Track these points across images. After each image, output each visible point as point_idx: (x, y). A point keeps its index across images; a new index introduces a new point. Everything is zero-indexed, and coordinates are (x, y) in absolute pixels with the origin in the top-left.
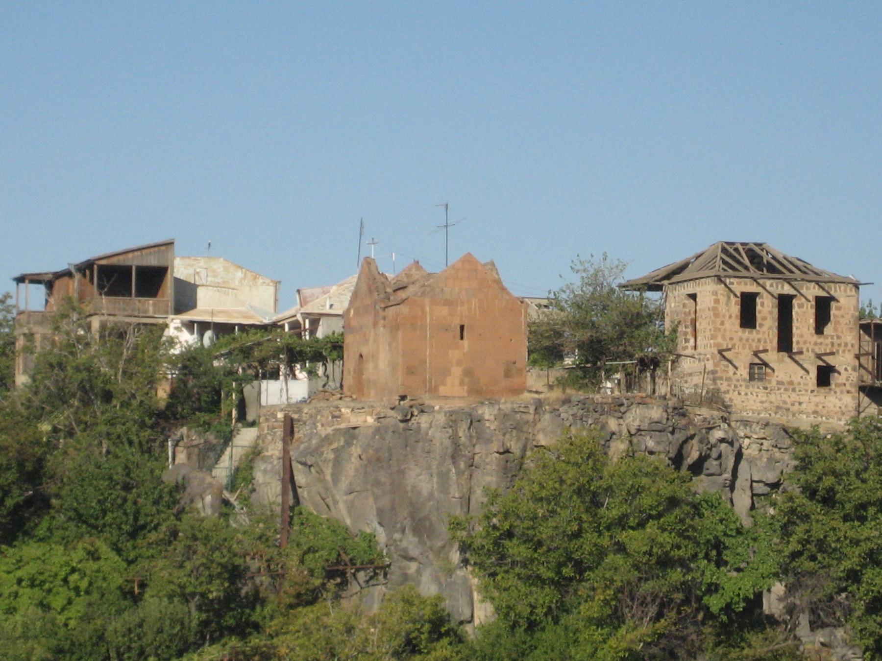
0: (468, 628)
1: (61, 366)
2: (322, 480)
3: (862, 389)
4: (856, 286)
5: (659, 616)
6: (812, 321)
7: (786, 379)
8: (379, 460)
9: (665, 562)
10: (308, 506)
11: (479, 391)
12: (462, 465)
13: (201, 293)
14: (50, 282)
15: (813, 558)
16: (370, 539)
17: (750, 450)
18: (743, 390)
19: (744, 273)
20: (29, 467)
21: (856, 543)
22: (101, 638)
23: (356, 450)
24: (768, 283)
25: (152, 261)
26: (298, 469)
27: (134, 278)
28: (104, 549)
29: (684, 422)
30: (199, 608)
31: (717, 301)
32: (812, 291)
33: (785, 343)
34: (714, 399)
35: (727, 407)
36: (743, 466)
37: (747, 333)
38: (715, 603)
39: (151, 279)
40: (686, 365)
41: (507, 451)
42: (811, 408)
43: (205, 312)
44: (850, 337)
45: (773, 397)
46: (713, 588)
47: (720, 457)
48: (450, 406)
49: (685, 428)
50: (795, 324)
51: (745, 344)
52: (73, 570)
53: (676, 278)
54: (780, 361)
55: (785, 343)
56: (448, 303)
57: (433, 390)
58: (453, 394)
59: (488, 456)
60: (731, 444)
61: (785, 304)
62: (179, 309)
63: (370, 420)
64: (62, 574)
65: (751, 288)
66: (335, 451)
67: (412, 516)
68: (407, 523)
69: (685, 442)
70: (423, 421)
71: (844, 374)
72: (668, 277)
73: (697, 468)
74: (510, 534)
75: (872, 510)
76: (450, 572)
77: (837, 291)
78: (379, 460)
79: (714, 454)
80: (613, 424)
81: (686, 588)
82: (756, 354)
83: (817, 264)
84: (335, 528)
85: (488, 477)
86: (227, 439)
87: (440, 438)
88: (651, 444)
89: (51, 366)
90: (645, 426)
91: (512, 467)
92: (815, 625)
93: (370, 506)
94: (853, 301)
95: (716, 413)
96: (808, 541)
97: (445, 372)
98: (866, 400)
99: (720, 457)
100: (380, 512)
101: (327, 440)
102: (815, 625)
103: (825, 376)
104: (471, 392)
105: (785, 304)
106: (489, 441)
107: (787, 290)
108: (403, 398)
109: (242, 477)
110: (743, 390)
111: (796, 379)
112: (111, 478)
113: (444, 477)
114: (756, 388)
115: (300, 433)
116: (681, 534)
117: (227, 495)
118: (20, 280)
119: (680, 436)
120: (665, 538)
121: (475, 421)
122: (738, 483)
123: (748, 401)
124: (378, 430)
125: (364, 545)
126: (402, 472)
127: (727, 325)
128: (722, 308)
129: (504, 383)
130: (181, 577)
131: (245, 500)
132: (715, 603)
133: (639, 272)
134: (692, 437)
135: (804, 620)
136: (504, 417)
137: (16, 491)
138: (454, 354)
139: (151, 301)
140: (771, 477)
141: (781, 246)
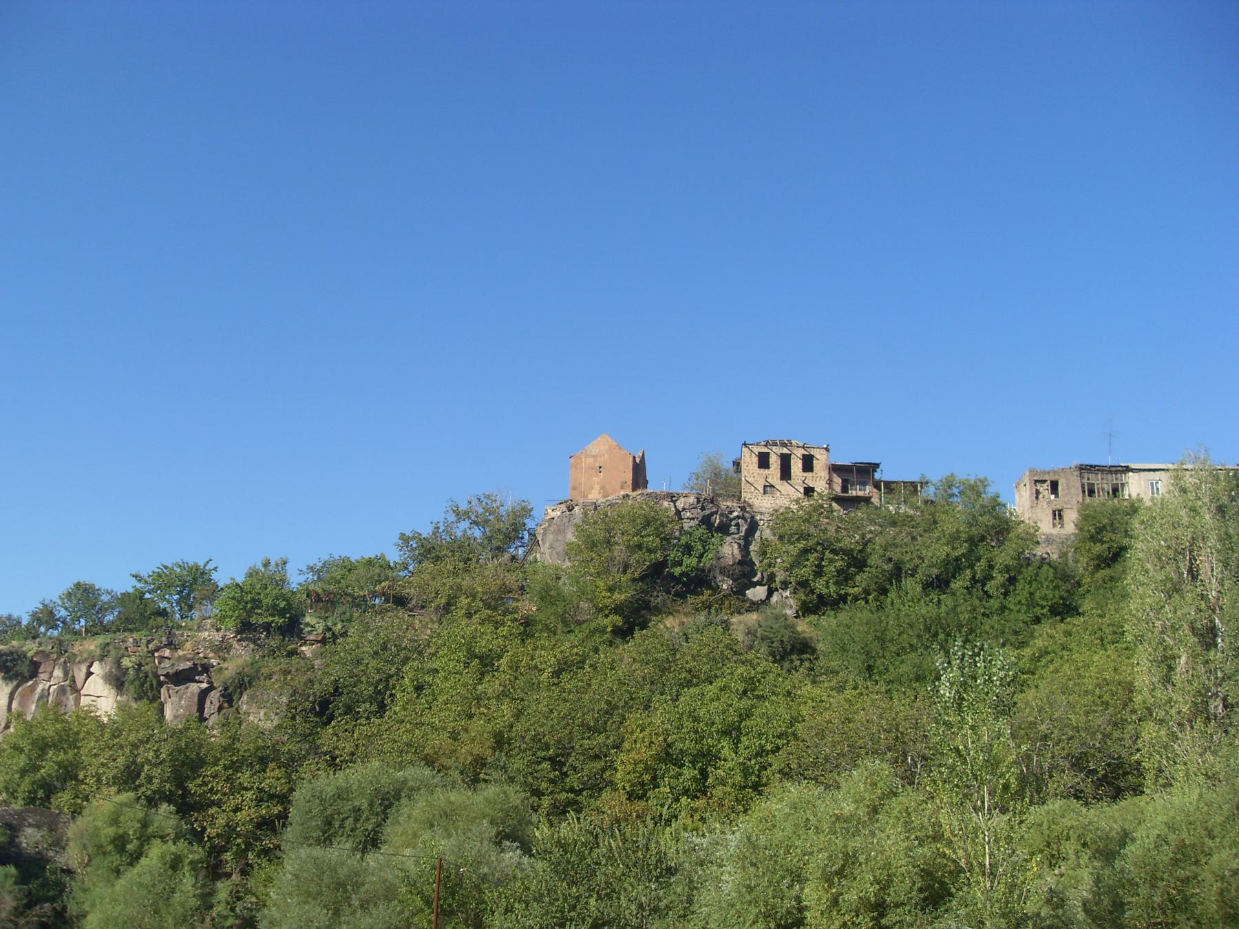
6: (800, 465)
32: (802, 452)
55: (786, 474)
57: (585, 496)
60: (743, 518)
61: (785, 461)
73: (724, 529)
98: (834, 504)
99: (737, 525)
105: (785, 461)
107: (785, 451)
114: (767, 497)
119: (707, 512)
134: (716, 513)
138: (596, 479)
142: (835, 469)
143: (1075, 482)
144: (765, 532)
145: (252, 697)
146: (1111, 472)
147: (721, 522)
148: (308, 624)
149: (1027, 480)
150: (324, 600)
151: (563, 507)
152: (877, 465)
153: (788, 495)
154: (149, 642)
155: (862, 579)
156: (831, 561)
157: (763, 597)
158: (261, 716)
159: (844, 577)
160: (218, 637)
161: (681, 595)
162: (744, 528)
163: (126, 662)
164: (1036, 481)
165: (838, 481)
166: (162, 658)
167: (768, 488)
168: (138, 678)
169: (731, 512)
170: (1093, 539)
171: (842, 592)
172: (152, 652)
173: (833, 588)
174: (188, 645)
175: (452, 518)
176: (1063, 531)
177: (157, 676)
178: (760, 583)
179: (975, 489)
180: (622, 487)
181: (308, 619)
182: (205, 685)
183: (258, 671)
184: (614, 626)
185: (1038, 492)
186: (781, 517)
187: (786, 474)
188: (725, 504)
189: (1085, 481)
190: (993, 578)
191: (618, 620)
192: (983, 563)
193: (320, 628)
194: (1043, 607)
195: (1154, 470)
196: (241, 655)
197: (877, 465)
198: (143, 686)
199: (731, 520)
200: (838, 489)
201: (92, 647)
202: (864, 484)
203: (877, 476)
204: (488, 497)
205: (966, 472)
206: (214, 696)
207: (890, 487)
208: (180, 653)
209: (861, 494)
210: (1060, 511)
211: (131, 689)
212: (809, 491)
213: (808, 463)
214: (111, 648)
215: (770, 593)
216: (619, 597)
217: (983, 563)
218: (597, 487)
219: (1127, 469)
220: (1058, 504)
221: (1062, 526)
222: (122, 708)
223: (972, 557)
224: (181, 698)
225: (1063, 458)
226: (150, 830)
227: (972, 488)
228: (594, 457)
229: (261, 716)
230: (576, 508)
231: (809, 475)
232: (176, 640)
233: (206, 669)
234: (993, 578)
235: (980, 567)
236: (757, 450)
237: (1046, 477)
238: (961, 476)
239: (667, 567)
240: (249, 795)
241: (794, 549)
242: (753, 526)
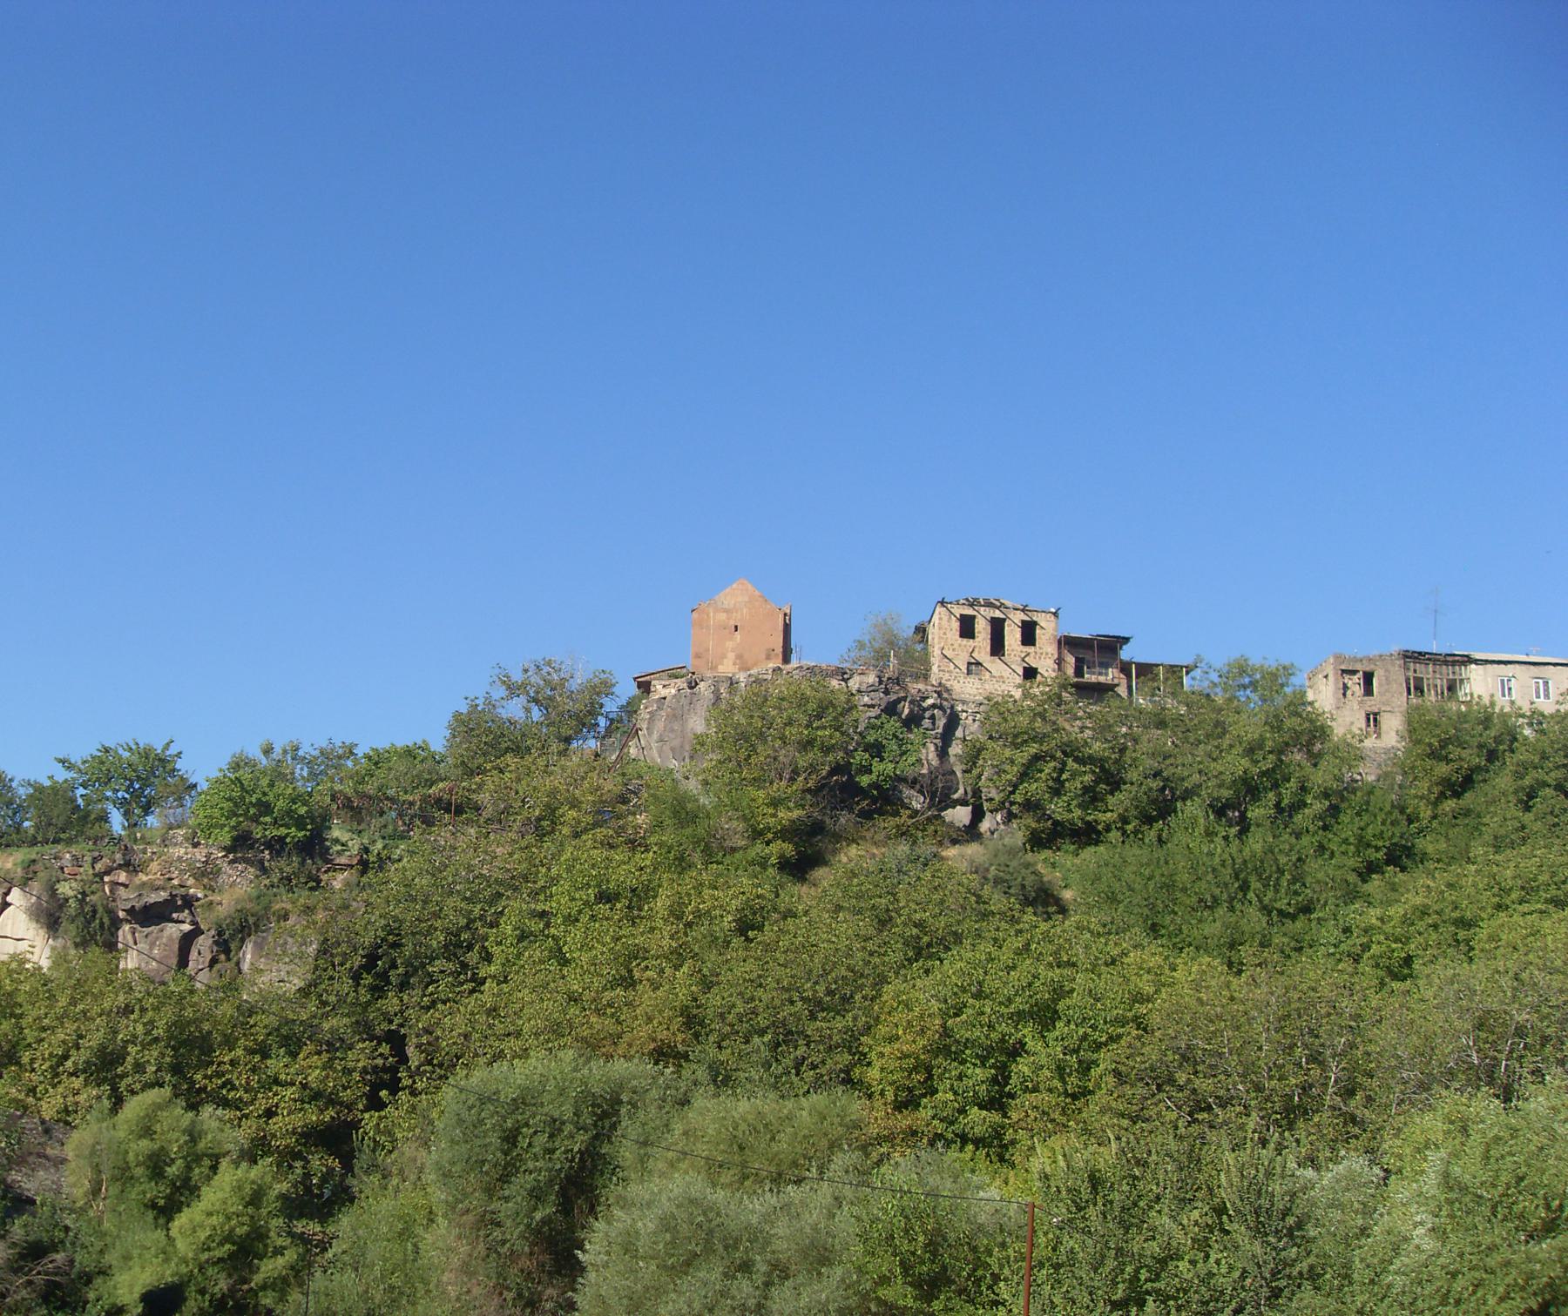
6: (1019, 636)
32: (1019, 617)
37: (965, 641)
38: (865, 780)
44: (1052, 650)
46: (868, 770)
55: (997, 647)
56: (726, 611)
57: (714, 668)
60: (941, 708)
61: (997, 627)
77: (1040, 619)
90: (863, 688)
93: (666, 748)
97: (723, 656)
99: (933, 717)
105: (997, 627)
107: (998, 614)
114: (971, 679)
119: (893, 697)
123: (967, 690)
127: (949, 635)
132: (865, 780)
134: (904, 699)
138: (729, 644)
142: (1067, 643)
143: (1398, 675)
144: (970, 727)
145: (259, 946)
146: (1446, 663)
147: (911, 711)
148: (337, 841)
149: (1330, 670)
150: (355, 810)
151: (682, 683)
152: (1126, 640)
153: (1003, 679)
154: (95, 860)
155: (1119, 802)
156: (1074, 775)
157: (966, 820)
158: (273, 973)
159: (1091, 797)
160: (200, 854)
161: (867, 815)
162: (941, 722)
163: (65, 889)
164: (1343, 671)
165: (1070, 659)
166: (115, 884)
167: (974, 666)
168: (81, 912)
169: (924, 699)
170: (1436, 755)
171: (1089, 818)
172: (101, 875)
173: (1078, 812)
174: (154, 866)
175: (501, 692)
176: (1379, 744)
177: (111, 913)
178: (964, 803)
179: (1274, 680)
180: (768, 658)
181: (336, 833)
182: (187, 927)
183: (267, 908)
184: (781, 856)
185: (1345, 687)
186: (996, 707)
187: (997, 647)
188: (915, 687)
189: (1411, 674)
190: (1305, 805)
191: (788, 849)
192: (1293, 784)
193: (355, 846)
194: (1377, 849)
195: (1487, 662)
196: (237, 886)
197: (1126, 640)
198: (89, 925)
199: (925, 710)
200: (1070, 671)
201: (9, 865)
202: (1106, 666)
203: (1126, 654)
204: (549, 664)
205: (1263, 656)
206: (204, 944)
207: (1146, 670)
208: (143, 877)
209: (1102, 679)
210: (1375, 714)
211: (70, 929)
212: (1030, 673)
213: (1029, 634)
214: (39, 867)
215: (978, 815)
216: (787, 815)
217: (1293, 784)
218: (731, 656)
219: (1468, 660)
220: (1372, 704)
221: (1379, 737)
222: (59, 959)
223: (1276, 777)
224: (152, 945)
225: (1381, 641)
226: (201, 1145)
227: (1274, 676)
228: (726, 611)
229: (273, 973)
230: (702, 685)
232: (136, 860)
233: (189, 902)
234: (1305, 805)
235: (1288, 792)
236: (959, 611)
237: (1358, 667)
238: (1255, 660)
239: (843, 776)
240: (289, 1092)
241: (1022, 757)
242: (953, 721)
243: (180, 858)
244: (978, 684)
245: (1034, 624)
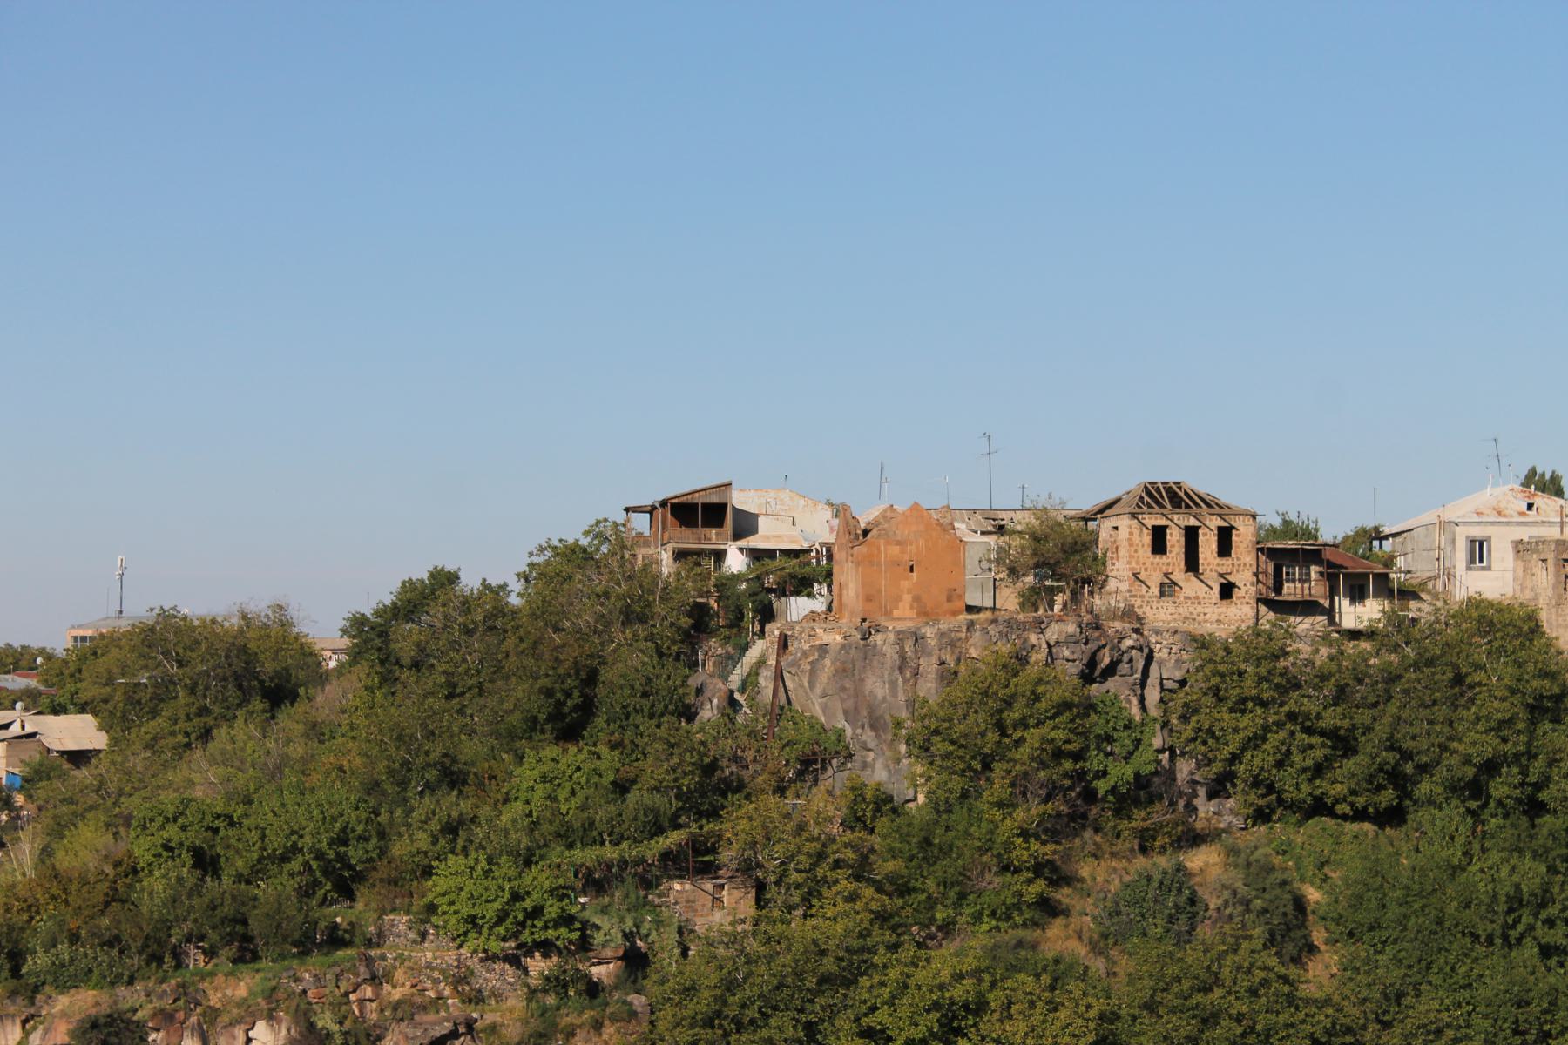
0: (911, 805)
1: (606, 595)
2: (802, 686)
3: (1261, 600)
4: (1254, 517)
5: (1048, 798)
6: (1214, 546)
7: (1192, 594)
8: (844, 670)
9: (1058, 755)
10: (796, 706)
11: (926, 614)
12: (908, 675)
13: (761, 521)
14: (652, 510)
15: (1205, 743)
16: (840, 734)
17: (1161, 653)
18: (1155, 605)
19: (1157, 509)
20: (583, 675)
21: (1236, 730)
22: (592, 824)
23: (828, 662)
24: (1176, 517)
25: (714, 499)
26: (786, 675)
27: (700, 512)
28: (603, 749)
29: (1097, 634)
30: (677, 797)
31: (1131, 534)
32: (1215, 522)
33: (1192, 564)
34: (1129, 614)
35: (1140, 620)
36: (1154, 668)
37: (1157, 558)
39: (714, 513)
40: (1112, 585)
41: (942, 663)
42: (1215, 617)
43: (767, 538)
44: (1249, 559)
45: (1181, 610)
46: (1105, 773)
47: (1131, 660)
48: (901, 626)
49: (1098, 639)
50: (1200, 550)
51: (1155, 568)
52: (579, 769)
53: (1108, 512)
54: (1188, 580)
55: (1192, 564)
56: (899, 543)
57: (888, 614)
58: (904, 616)
59: (929, 666)
60: (1141, 649)
61: (1191, 534)
62: (737, 536)
63: (839, 638)
64: (569, 772)
65: (1162, 522)
66: (812, 663)
67: (870, 714)
68: (866, 721)
69: (1098, 650)
70: (878, 638)
71: (1244, 589)
72: (1101, 511)
73: (1111, 670)
74: (936, 732)
75: (1250, 705)
76: (898, 761)
78: (844, 670)
79: (1126, 658)
80: (1033, 638)
81: (1080, 775)
82: (1166, 575)
83: (1224, 499)
84: (813, 723)
85: (928, 687)
86: (745, 648)
87: (890, 652)
88: (1067, 653)
89: (598, 596)
90: (1062, 638)
91: (948, 676)
92: (1211, 796)
94: (1251, 529)
95: (1127, 626)
96: (1200, 730)
97: (898, 599)
98: (1263, 609)
99: (1131, 660)
100: (846, 712)
101: (805, 654)
102: (1211, 796)
103: (1227, 591)
104: (919, 614)
105: (1191, 534)
106: (930, 655)
107: (1193, 522)
108: (864, 620)
109: (749, 683)
110: (1155, 605)
111: (1201, 594)
112: (632, 687)
113: (893, 684)
114: (1167, 603)
115: (793, 646)
116: (1071, 731)
117: (737, 696)
118: (627, 510)
119: (1092, 646)
120: (1060, 735)
121: (918, 639)
122: (1149, 681)
123: (1159, 614)
124: (843, 647)
125: (833, 738)
126: (862, 680)
127: (1140, 552)
128: (1136, 538)
129: (947, 606)
130: (660, 773)
131: (751, 699)
133: (1087, 504)
135: (1202, 792)
136: (942, 635)
137: (576, 694)
138: (905, 584)
139: (714, 531)
140: (1178, 675)
141: (1196, 481)
144: (1168, 667)
160: (450, 957)
162: (1140, 665)
166: (361, 1001)
167: (1168, 588)
169: (1121, 640)
171: (1317, 792)
172: (346, 995)
174: (399, 975)
214: (281, 995)
218: (907, 598)
231: (1226, 562)
232: (380, 967)
243: (428, 966)
244: (1172, 608)
245: (1232, 528)
